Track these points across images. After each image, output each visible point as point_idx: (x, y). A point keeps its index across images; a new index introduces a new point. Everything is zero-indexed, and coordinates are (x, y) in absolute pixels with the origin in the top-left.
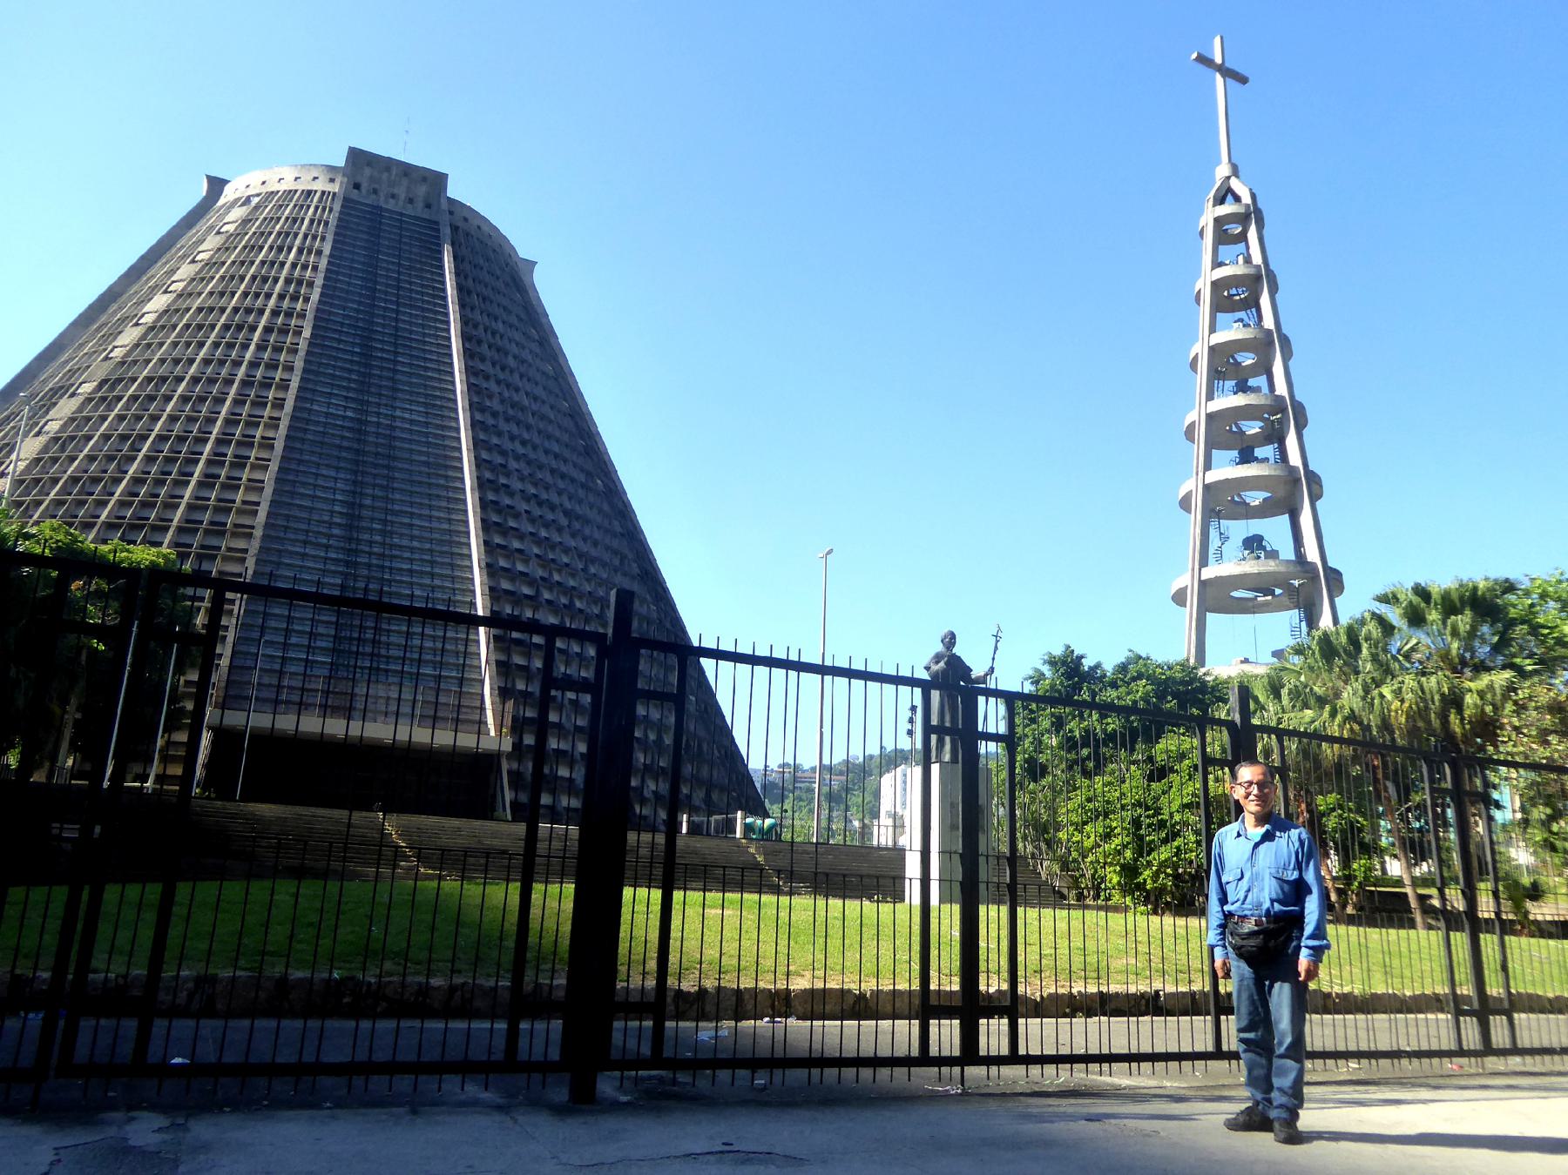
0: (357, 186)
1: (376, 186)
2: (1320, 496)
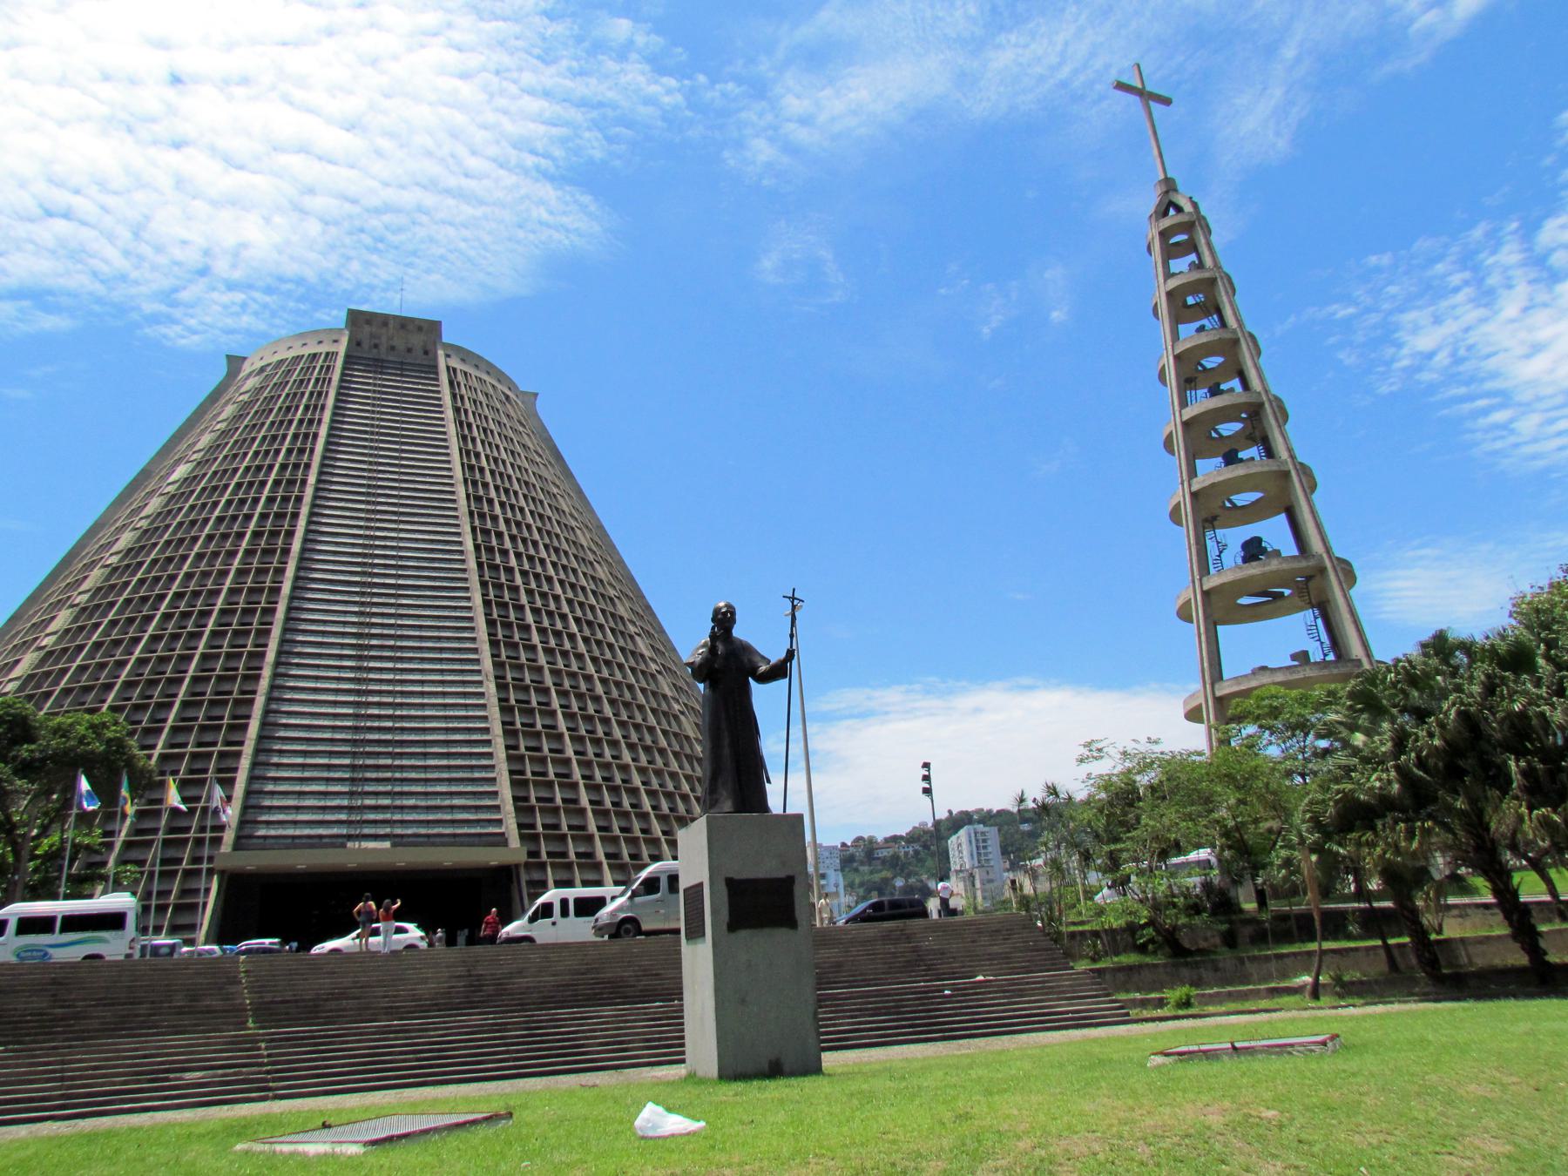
1: (377, 341)
2: (1313, 487)
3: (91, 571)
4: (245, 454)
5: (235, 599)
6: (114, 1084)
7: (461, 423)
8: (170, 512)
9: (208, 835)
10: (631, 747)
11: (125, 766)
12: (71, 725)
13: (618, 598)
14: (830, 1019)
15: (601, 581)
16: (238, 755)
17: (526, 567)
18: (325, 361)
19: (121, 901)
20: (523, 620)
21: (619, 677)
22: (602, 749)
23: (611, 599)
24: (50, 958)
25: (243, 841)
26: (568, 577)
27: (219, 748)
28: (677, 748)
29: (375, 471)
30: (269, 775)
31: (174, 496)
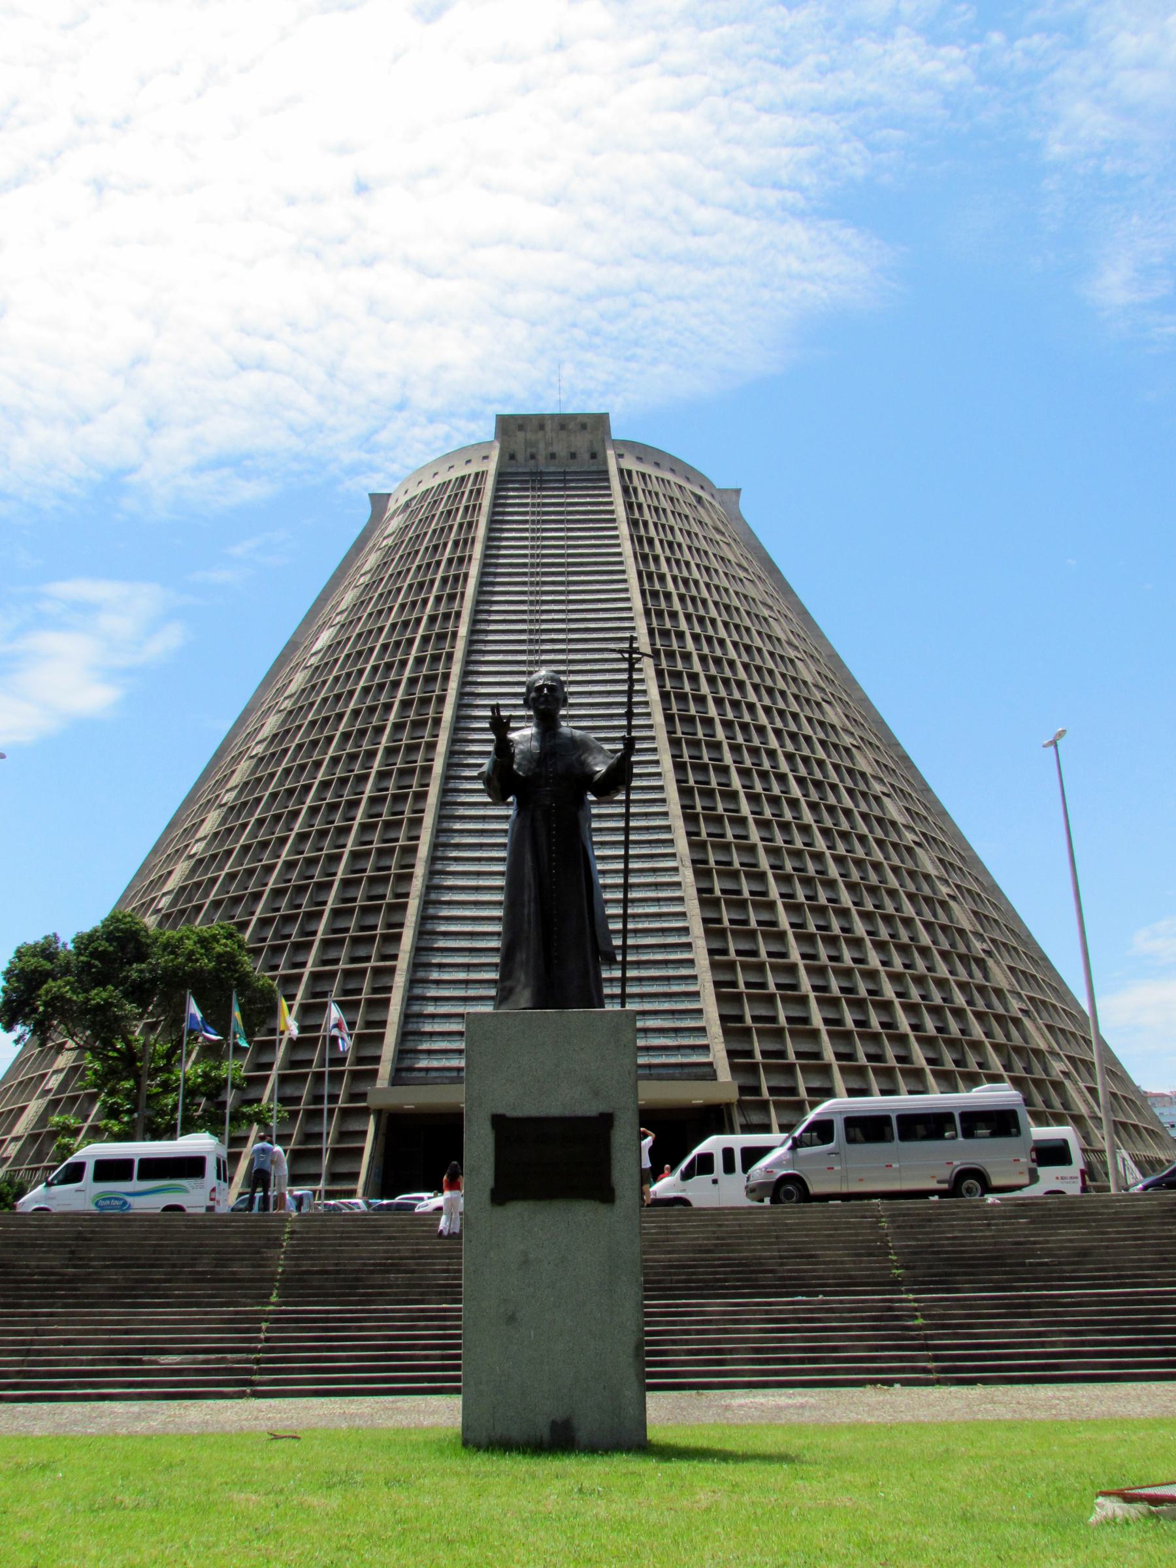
0: (512, 457)
1: (534, 450)
3: (239, 764)
4: (391, 609)
5: (384, 785)
6: (81, 1363)
7: (640, 539)
8: (314, 687)
9: (327, 1069)
10: (880, 946)
11: (237, 986)
12: (181, 939)
13: (858, 748)
14: (1039, 1334)
15: (833, 727)
16: (392, 970)
17: (730, 715)
18: (474, 483)
19: (199, 1143)
20: (728, 785)
21: (860, 853)
22: (839, 949)
23: (847, 750)
24: (129, 1208)
25: (404, 1074)
26: (786, 725)
27: (373, 963)
28: (946, 946)
29: (537, 611)
30: (429, 994)
31: (317, 668)
